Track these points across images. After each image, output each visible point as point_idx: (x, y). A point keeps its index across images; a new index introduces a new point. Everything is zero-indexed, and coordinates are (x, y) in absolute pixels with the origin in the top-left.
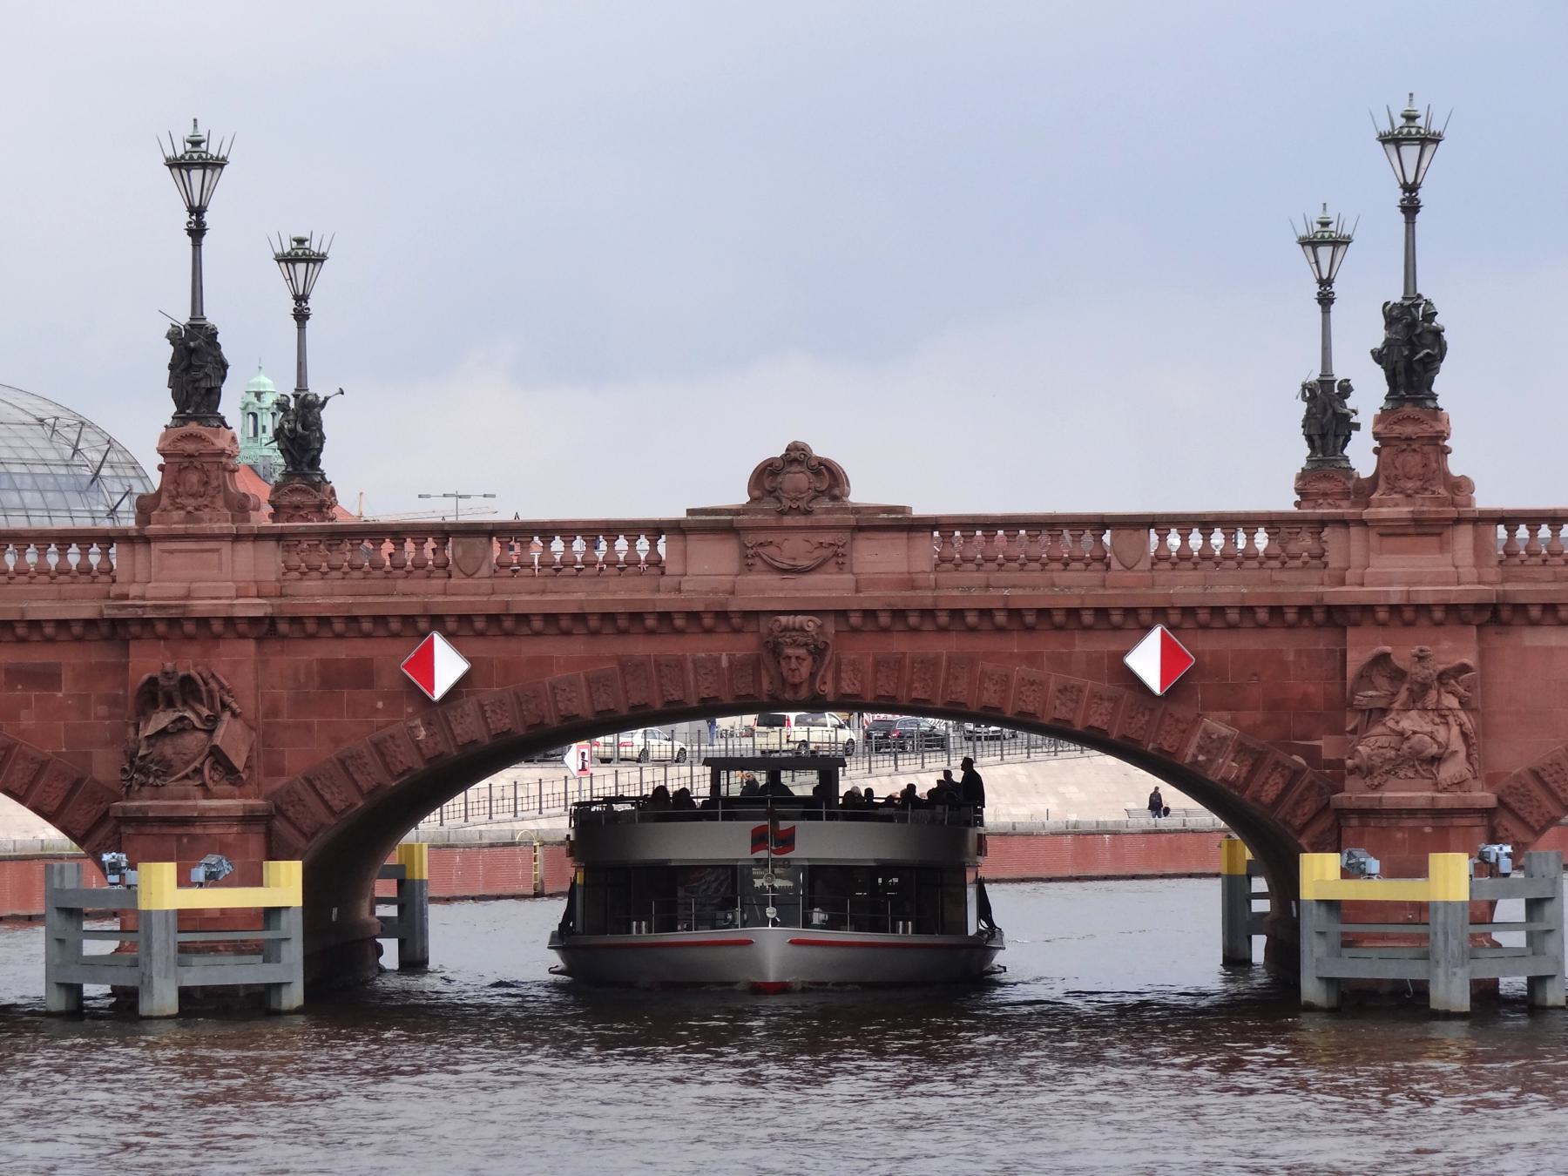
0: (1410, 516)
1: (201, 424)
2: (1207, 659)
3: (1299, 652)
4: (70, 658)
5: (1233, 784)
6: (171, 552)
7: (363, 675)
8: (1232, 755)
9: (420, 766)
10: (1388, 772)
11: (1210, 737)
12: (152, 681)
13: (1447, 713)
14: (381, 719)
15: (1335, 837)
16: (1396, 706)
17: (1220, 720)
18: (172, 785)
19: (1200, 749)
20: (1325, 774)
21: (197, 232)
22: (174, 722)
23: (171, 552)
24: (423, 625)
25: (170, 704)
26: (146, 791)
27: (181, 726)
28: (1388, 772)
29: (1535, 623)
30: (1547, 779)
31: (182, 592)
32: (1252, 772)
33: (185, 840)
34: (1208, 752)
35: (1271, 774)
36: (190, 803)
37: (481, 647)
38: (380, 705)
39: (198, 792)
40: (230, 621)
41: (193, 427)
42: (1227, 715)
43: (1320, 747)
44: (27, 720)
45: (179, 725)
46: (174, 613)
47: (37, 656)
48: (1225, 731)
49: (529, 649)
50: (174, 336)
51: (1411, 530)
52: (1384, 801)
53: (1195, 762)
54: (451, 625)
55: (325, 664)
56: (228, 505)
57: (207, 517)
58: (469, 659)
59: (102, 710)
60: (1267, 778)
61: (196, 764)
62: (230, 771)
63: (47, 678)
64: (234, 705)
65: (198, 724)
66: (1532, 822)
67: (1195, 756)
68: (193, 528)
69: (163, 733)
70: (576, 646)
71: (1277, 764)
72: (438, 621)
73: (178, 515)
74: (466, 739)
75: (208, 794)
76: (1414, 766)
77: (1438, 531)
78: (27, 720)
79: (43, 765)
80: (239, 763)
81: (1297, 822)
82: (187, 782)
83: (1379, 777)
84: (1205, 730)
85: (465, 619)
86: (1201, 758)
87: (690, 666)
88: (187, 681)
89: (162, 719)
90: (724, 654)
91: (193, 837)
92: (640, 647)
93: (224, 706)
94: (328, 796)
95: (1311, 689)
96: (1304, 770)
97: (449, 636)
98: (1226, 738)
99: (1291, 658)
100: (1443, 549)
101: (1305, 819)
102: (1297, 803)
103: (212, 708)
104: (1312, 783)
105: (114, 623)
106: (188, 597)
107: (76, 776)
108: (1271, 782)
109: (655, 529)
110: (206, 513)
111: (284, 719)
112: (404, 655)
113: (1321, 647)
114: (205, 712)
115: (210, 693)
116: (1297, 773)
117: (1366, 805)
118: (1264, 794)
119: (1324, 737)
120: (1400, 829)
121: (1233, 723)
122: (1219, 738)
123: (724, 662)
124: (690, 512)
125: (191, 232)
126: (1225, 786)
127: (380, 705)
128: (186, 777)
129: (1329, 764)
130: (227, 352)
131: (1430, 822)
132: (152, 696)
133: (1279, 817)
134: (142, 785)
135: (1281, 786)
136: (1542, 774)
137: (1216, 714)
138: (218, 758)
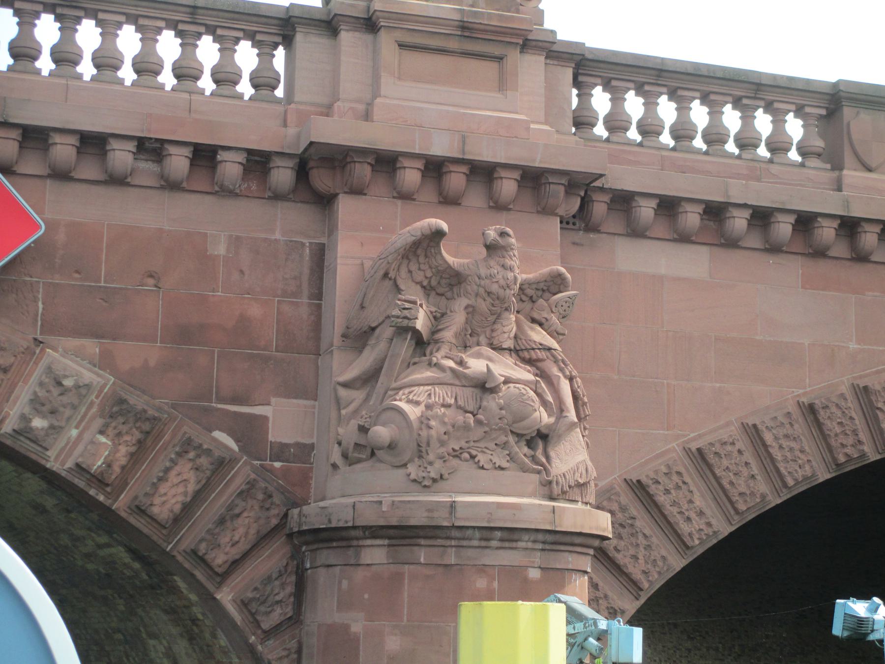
0: (457, 17)
2: (61, 237)
3: (236, 242)
5: (99, 481)
8: (99, 423)
10: (456, 454)
11: (59, 384)
13: (541, 354)
15: (290, 589)
16: (448, 335)
17: (78, 354)
19: (37, 404)
20: (271, 470)
28: (456, 454)
29: (636, 232)
30: (661, 499)
32: (136, 458)
34: (53, 412)
35: (174, 462)
42: (92, 347)
43: (265, 419)
48: (88, 376)
51: (453, 45)
52: (458, 509)
53: (24, 432)
60: (167, 470)
66: (637, 575)
67: (24, 418)
71: (188, 444)
76: (505, 445)
77: (496, 51)
81: (219, 559)
83: (438, 464)
84: (49, 370)
86: (38, 423)
95: (255, 311)
96: (233, 461)
98: (88, 386)
99: (221, 250)
100: (503, 84)
101: (235, 553)
102: (222, 521)
104: (252, 484)
108: (173, 477)
113: (278, 236)
116: (222, 465)
117: (418, 518)
118: (157, 500)
119: (273, 400)
120: (483, 569)
121: (105, 362)
122: (77, 387)
126: (81, 483)
129: (280, 451)
131: (537, 558)
133: (183, 546)
135: (192, 487)
136: (653, 489)
137: (73, 343)
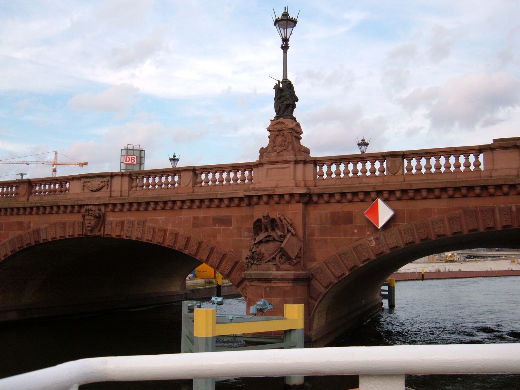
1: (284, 118)
4: (235, 213)
6: (271, 169)
7: (349, 218)
9: (373, 257)
12: (259, 220)
14: (356, 237)
18: (264, 265)
21: (285, 48)
22: (266, 237)
23: (271, 169)
24: (373, 195)
25: (267, 230)
26: (254, 267)
27: (268, 240)
31: (274, 185)
33: (268, 289)
36: (269, 272)
37: (400, 205)
38: (356, 231)
39: (274, 268)
40: (292, 195)
41: (281, 119)
44: (220, 238)
45: (268, 239)
46: (270, 193)
47: (223, 212)
49: (420, 205)
50: (277, 87)
54: (386, 195)
55: (333, 214)
56: (293, 149)
57: (285, 154)
58: (394, 210)
59: (246, 234)
61: (274, 256)
62: (289, 258)
63: (226, 221)
64: (293, 231)
65: (276, 238)
68: (280, 159)
69: (261, 242)
70: (443, 203)
72: (379, 193)
73: (274, 154)
74: (393, 246)
75: (278, 269)
78: (220, 238)
79: (224, 256)
80: (293, 256)
82: (269, 263)
85: (392, 192)
87: (497, 211)
88: (273, 221)
89: (262, 236)
90: (514, 205)
91: (271, 288)
92: (472, 203)
93: (289, 231)
94: (333, 270)
97: (386, 201)
103: (284, 232)
105: (250, 197)
106: (276, 187)
107: (236, 260)
109: (478, 150)
110: (285, 153)
111: (316, 237)
112: (365, 207)
114: (280, 233)
115: (283, 226)
123: (514, 209)
124: (495, 141)
125: (283, 48)
127: (356, 231)
128: (269, 261)
130: (297, 93)
132: (258, 226)
134: (252, 264)
138: (283, 253)
